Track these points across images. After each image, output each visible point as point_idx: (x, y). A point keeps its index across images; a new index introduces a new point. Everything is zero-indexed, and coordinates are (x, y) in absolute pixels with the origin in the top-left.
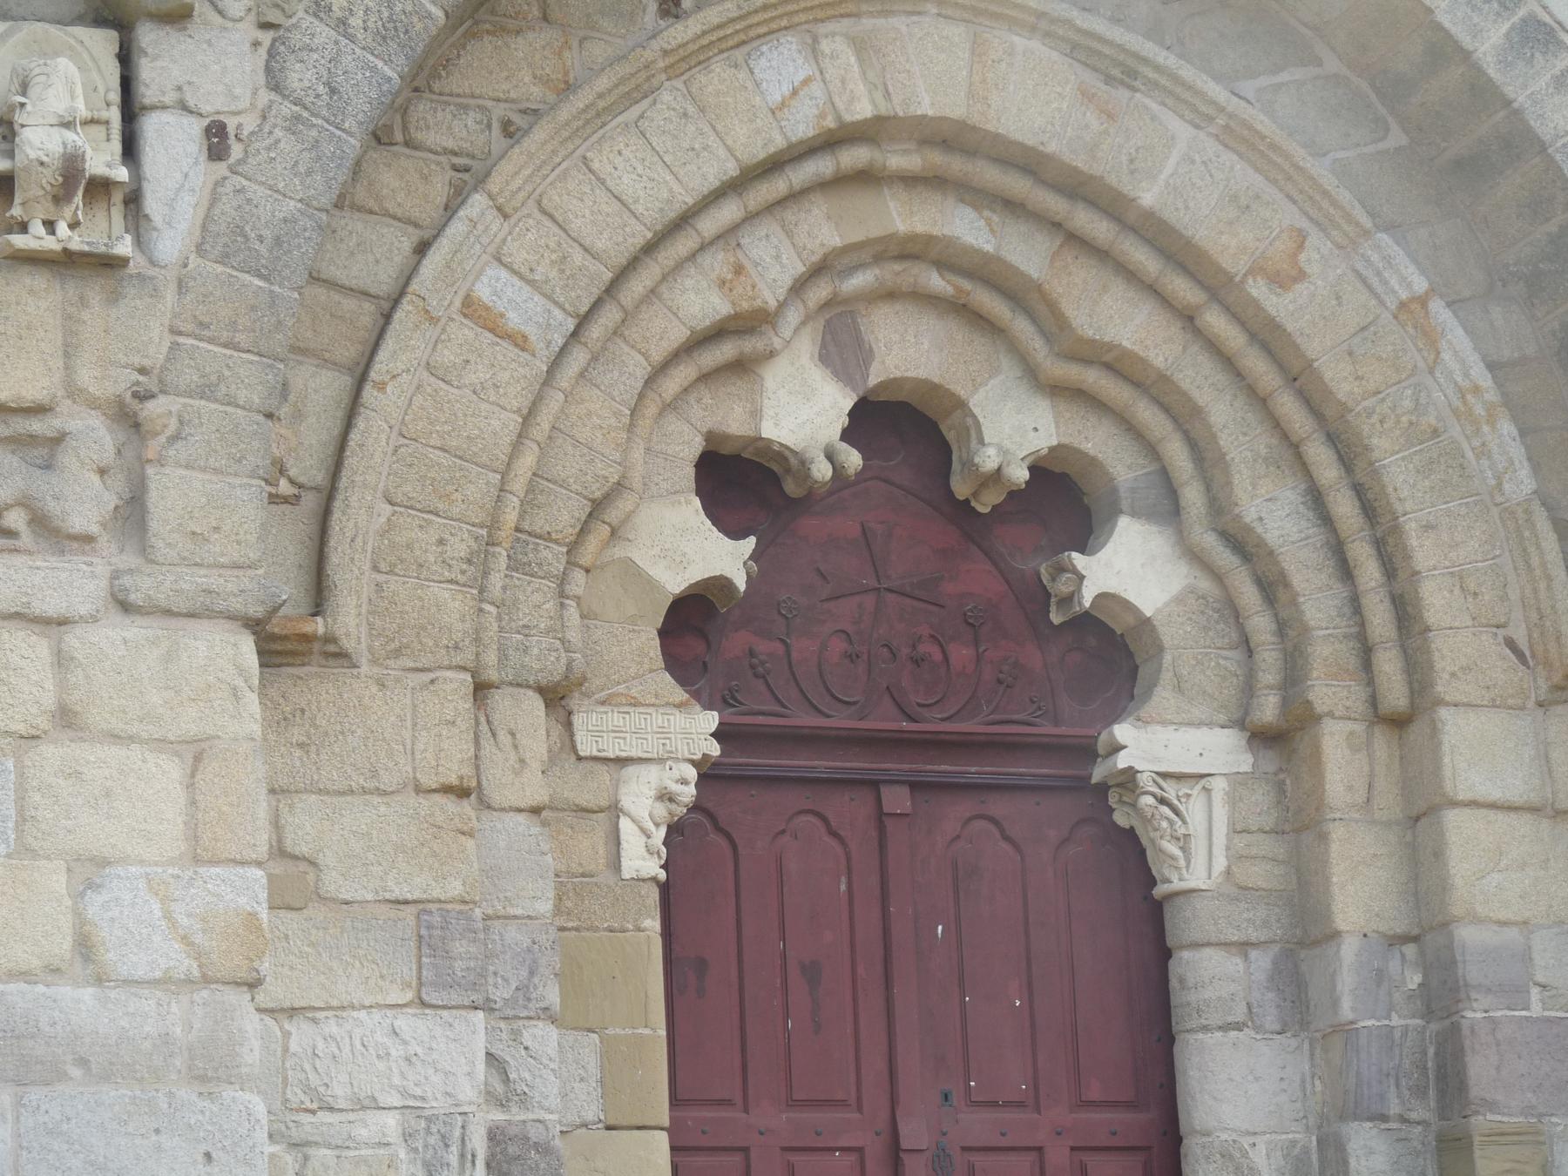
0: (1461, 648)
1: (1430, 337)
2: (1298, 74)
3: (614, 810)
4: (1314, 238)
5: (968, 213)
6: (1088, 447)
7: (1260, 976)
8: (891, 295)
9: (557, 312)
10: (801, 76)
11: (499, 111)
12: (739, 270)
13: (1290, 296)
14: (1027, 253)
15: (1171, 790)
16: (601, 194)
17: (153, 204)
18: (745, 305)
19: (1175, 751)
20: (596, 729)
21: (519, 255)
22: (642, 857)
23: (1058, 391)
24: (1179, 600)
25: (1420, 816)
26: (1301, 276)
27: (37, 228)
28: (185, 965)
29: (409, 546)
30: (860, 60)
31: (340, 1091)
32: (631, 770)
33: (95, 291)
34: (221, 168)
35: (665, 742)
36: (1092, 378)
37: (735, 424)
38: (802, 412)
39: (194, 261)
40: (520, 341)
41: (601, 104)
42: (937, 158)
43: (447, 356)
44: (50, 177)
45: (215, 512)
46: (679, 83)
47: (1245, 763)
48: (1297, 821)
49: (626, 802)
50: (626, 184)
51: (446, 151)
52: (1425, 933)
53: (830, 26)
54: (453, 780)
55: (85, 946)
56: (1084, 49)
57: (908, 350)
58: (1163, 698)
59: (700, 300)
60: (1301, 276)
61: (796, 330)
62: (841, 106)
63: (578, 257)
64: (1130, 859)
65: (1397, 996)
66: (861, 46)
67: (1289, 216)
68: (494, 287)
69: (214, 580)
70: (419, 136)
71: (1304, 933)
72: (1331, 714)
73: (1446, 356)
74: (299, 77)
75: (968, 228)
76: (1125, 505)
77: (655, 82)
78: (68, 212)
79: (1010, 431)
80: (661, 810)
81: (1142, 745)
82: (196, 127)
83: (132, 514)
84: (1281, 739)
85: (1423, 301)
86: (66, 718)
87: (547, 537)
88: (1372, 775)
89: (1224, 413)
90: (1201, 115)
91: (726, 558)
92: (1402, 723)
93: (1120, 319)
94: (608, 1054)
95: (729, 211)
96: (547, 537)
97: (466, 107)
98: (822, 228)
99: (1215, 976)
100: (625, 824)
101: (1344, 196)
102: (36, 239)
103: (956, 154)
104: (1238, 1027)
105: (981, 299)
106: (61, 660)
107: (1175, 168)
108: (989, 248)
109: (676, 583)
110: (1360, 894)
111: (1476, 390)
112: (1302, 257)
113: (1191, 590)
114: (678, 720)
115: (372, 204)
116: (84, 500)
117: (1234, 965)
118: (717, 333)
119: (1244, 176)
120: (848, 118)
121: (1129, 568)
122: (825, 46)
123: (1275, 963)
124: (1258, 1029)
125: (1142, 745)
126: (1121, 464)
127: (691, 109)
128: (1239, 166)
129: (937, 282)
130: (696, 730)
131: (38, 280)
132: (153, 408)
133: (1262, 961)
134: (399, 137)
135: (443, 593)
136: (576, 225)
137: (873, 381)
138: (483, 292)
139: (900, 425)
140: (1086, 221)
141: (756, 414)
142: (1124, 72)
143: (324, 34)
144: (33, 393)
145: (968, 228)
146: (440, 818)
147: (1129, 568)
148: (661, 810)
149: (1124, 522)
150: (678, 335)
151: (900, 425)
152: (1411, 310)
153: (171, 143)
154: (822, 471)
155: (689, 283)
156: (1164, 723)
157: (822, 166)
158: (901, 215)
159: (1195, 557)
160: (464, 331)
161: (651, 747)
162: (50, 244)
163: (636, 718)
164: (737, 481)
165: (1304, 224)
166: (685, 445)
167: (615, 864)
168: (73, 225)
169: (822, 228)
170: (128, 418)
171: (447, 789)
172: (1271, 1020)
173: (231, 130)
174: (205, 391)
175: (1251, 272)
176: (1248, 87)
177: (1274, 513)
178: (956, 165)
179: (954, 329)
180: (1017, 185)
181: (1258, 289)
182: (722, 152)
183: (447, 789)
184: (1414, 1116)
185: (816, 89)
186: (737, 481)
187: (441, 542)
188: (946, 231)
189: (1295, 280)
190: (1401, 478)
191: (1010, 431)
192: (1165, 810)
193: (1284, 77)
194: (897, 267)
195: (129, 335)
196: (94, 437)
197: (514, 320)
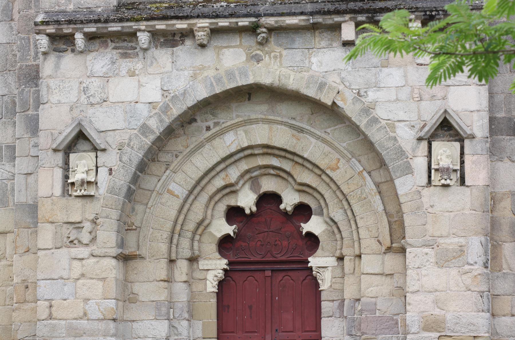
0: (369, 243)
1: (364, 178)
2: (340, 126)
3: (205, 279)
4: (342, 160)
5: (275, 159)
6: (306, 202)
7: (336, 307)
8: (266, 175)
9: (185, 190)
10: (234, 139)
11: (175, 153)
12: (227, 176)
13: (335, 173)
14: (287, 166)
15: (321, 270)
16: (194, 167)
17: (99, 184)
18: (228, 183)
20: (203, 264)
21: (177, 180)
22: (212, 287)
23: (299, 191)
24: (324, 232)
26: (338, 168)
27: (79, 191)
28: (102, 317)
29: (156, 237)
30: (246, 135)
31: (141, 335)
32: (210, 271)
33: (88, 200)
34: (111, 177)
35: (215, 266)
36: (304, 188)
37: (233, 203)
38: (247, 200)
39: (106, 194)
40: (177, 197)
41: (193, 150)
42: (265, 150)
43: (164, 200)
44: (79, 183)
45: (108, 237)
46: (209, 144)
47: (336, 264)
49: (208, 278)
50: (198, 164)
51: (165, 162)
53: (240, 128)
54: (163, 279)
55: (85, 314)
56: (292, 127)
57: (269, 185)
58: (319, 251)
59: (219, 182)
60: (338, 168)
61: (243, 185)
62: (241, 144)
63: (189, 179)
64: (315, 284)
65: (356, 311)
66: (246, 132)
67: (337, 156)
68: (173, 186)
69: (108, 250)
70: (160, 159)
72: (346, 255)
73: (367, 183)
74: (125, 158)
75: (275, 162)
76: (313, 213)
77: (204, 144)
78: (83, 188)
79: (290, 200)
80: (216, 279)
81: (314, 262)
82: (107, 169)
83: (94, 239)
84: (341, 259)
85: (362, 172)
86: (83, 275)
87: (188, 231)
88: (355, 267)
89: (327, 194)
90: (318, 138)
91: (230, 230)
93: (305, 177)
94: (203, 324)
95: (222, 166)
96: (188, 231)
97: (169, 153)
98: (244, 166)
100: (208, 282)
101: (345, 152)
102: (78, 193)
103: (268, 149)
104: (331, 317)
106: (83, 266)
107: (311, 148)
108: (279, 166)
109: (219, 235)
111: (372, 190)
112: (339, 164)
113: (327, 229)
114: (218, 262)
115: (151, 173)
116: (85, 238)
117: (331, 304)
118: (226, 187)
119: (327, 149)
120: (243, 147)
121: (314, 225)
122: (239, 133)
123: (339, 304)
124: (335, 317)
125: (314, 262)
126: (313, 205)
127: (211, 148)
128: (326, 146)
129: (272, 172)
130: (223, 263)
131: (79, 200)
132: (98, 221)
133: (336, 304)
134: (156, 160)
135: (161, 245)
136: (189, 173)
137: (261, 192)
138: (171, 188)
140: (296, 159)
141: (237, 201)
142: (301, 130)
143: (129, 149)
144: (78, 220)
145: (275, 162)
146: (160, 286)
147: (314, 225)
148: (216, 279)
149: (313, 216)
150: (214, 189)
152: (360, 173)
153: (103, 172)
154: (248, 212)
155: (217, 179)
156: (319, 257)
157: (241, 155)
158: (262, 161)
159: (326, 223)
160: (166, 196)
161: (213, 267)
162: (80, 194)
163: (210, 262)
164: (234, 214)
165: (340, 157)
166: (222, 208)
167: (206, 289)
168: (85, 190)
169: (244, 166)
170: (94, 222)
171: (162, 280)
172: (338, 316)
173: (113, 169)
174: (107, 217)
175: (327, 168)
176: (329, 130)
177: (338, 215)
178: (270, 151)
179: (279, 180)
180: (283, 154)
181: (328, 172)
182: (217, 156)
183: (162, 280)
184: (357, 335)
185: (236, 142)
186: (234, 214)
187: (161, 235)
188: (270, 163)
189: (337, 169)
190: (356, 208)
191: (290, 200)
192: (318, 274)
193: (337, 127)
194: (264, 170)
195: (91, 209)
196: (88, 226)
197: (176, 193)
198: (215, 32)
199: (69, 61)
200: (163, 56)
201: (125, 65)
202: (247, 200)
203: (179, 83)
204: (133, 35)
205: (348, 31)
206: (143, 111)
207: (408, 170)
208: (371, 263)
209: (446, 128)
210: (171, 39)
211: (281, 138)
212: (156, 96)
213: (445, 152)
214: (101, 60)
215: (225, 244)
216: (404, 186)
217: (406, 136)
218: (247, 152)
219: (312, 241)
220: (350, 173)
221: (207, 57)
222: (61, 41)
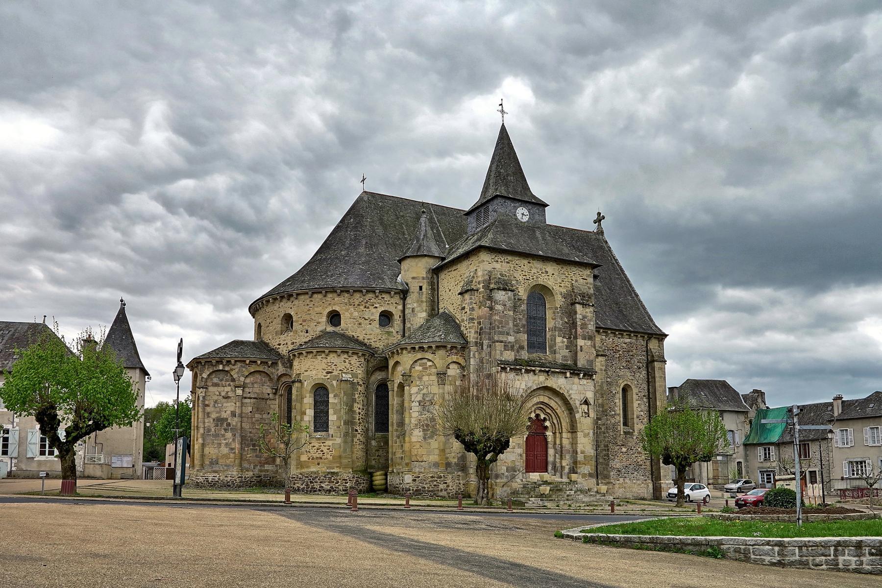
0: (564, 430)
19: (549, 433)
25: (561, 438)
48: (555, 438)
52: (561, 444)
57: (538, 412)
71: (555, 444)
79: (542, 416)
84: (554, 433)
92: (561, 433)
99: (550, 446)
105: (541, 409)
107: (552, 404)
110: (558, 442)
121: (547, 424)
125: (547, 433)
139: (537, 416)
147: (547, 424)
151: (537, 416)
177: (555, 422)
191: (542, 416)
198: (540, 371)
199: (503, 374)
200: (526, 375)
201: (517, 377)
202: (533, 415)
203: (530, 385)
204: (521, 370)
205: (568, 375)
206: (521, 391)
207: (578, 412)
208: (565, 435)
209: (586, 402)
210: (527, 371)
211: (546, 400)
212: (523, 386)
213: (585, 407)
214: (512, 375)
215: (528, 428)
216: (577, 416)
217: (578, 403)
218: (538, 403)
219: (546, 428)
220: (561, 411)
221: (536, 377)
222: (504, 369)
